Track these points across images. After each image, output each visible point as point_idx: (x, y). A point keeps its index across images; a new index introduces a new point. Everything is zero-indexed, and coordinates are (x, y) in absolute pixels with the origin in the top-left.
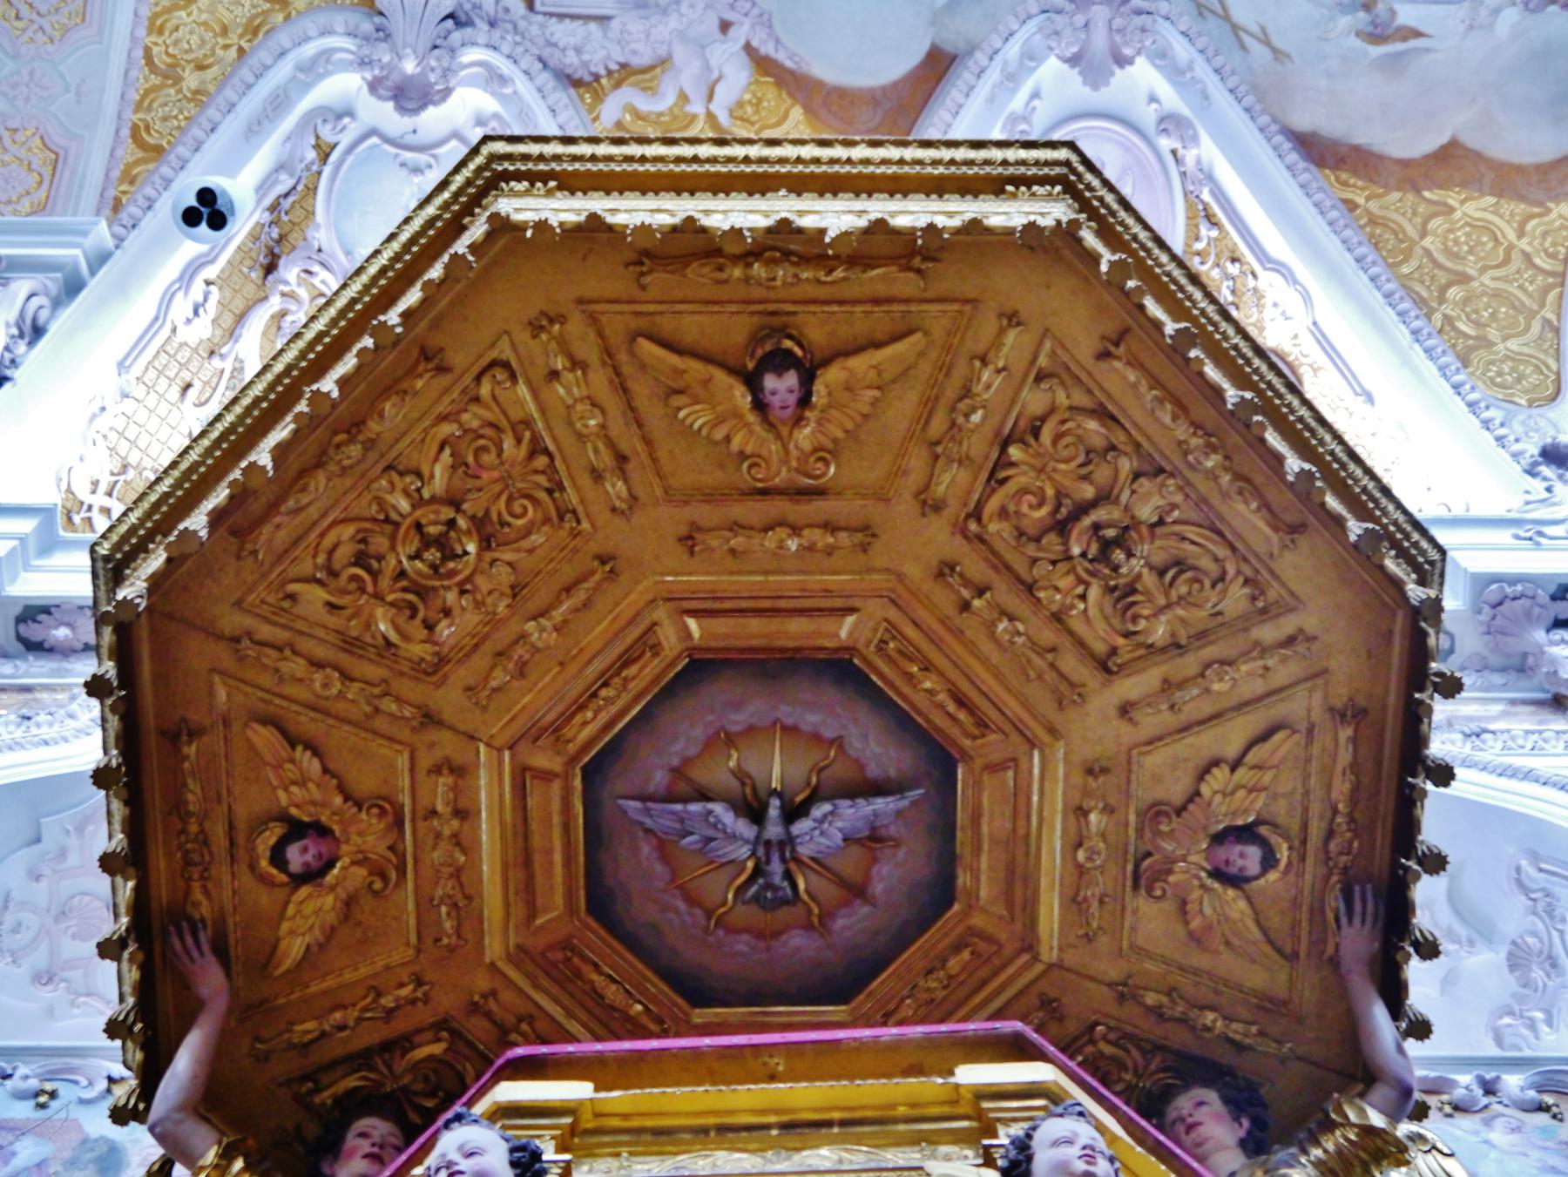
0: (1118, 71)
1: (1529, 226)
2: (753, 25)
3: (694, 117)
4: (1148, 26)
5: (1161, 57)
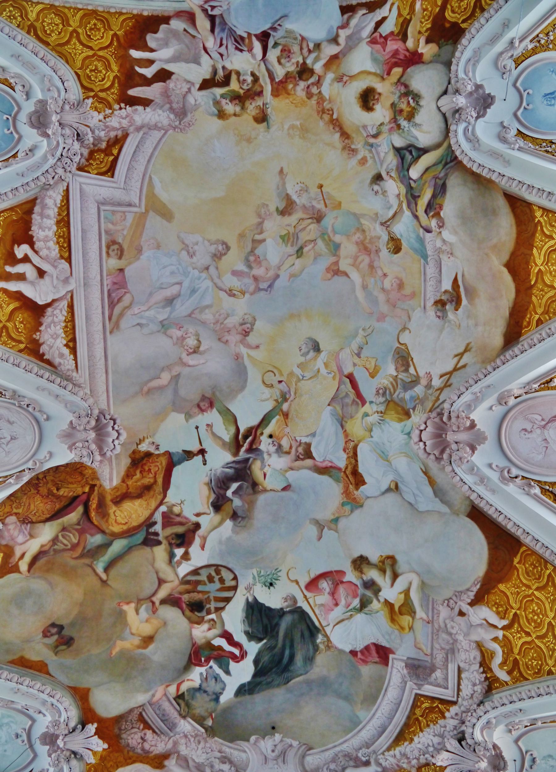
0: (478, 427)
1: (548, 233)
2: (460, 600)
3: (504, 636)
4: (456, 415)
5: (470, 407)
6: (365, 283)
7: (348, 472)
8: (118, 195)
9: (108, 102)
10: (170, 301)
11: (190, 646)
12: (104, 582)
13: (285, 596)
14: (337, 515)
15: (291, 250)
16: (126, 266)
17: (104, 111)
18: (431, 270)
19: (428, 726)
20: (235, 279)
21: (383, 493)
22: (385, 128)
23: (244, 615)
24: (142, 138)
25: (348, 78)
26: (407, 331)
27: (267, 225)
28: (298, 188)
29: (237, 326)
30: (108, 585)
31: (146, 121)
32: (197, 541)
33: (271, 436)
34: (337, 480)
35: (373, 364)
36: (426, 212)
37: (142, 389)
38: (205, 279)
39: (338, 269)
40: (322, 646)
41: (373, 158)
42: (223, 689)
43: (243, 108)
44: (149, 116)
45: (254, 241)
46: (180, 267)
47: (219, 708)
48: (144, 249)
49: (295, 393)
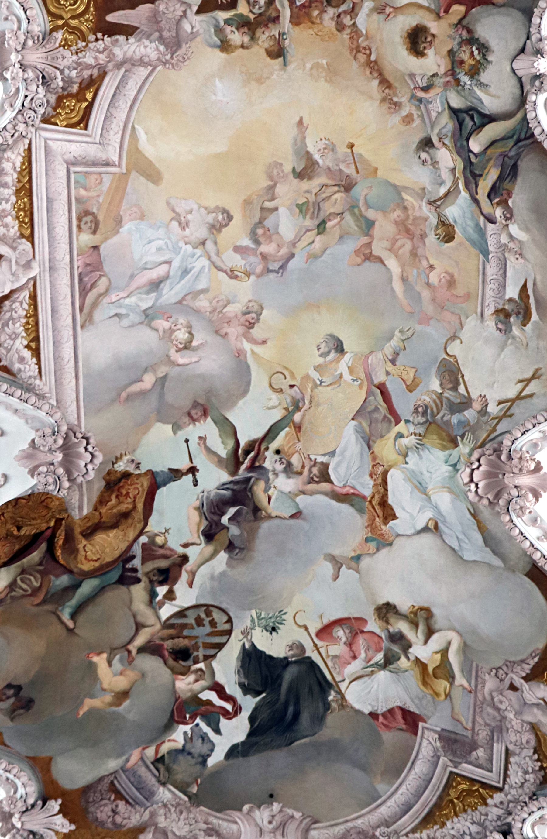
6: (405, 275)
7: (374, 503)
9: (81, 31)
11: (173, 700)
12: (70, 631)
13: (290, 643)
14: (358, 552)
16: (102, 242)
17: (77, 44)
19: (465, 811)
20: (238, 257)
21: (419, 532)
22: (440, 81)
23: (240, 664)
24: (123, 76)
25: (391, 10)
26: (458, 341)
27: (280, 189)
28: (321, 145)
29: (239, 316)
30: (76, 634)
31: (130, 53)
32: (184, 577)
33: (278, 452)
34: (361, 511)
35: (412, 375)
36: (489, 196)
37: (119, 395)
38: (200, 256)
39: (371, 253)
40: (334, 705)
41: (421, 116)
42: (212, 750)
43: (253, 38)
44: (133, 48)
45: (262, 209)
46: (168, 241)
47: (206, 772)
48: (125, 219)
49: (311, 402)
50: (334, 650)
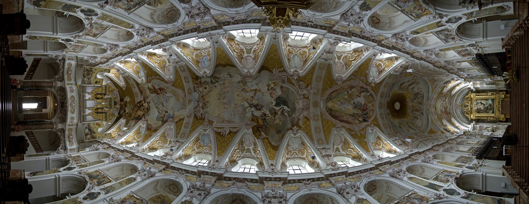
8: (216, 121)
10: (231, 115)
15: (225, 98)
18: (227, 78)
34: (256, 93)
50: (274, 96)
